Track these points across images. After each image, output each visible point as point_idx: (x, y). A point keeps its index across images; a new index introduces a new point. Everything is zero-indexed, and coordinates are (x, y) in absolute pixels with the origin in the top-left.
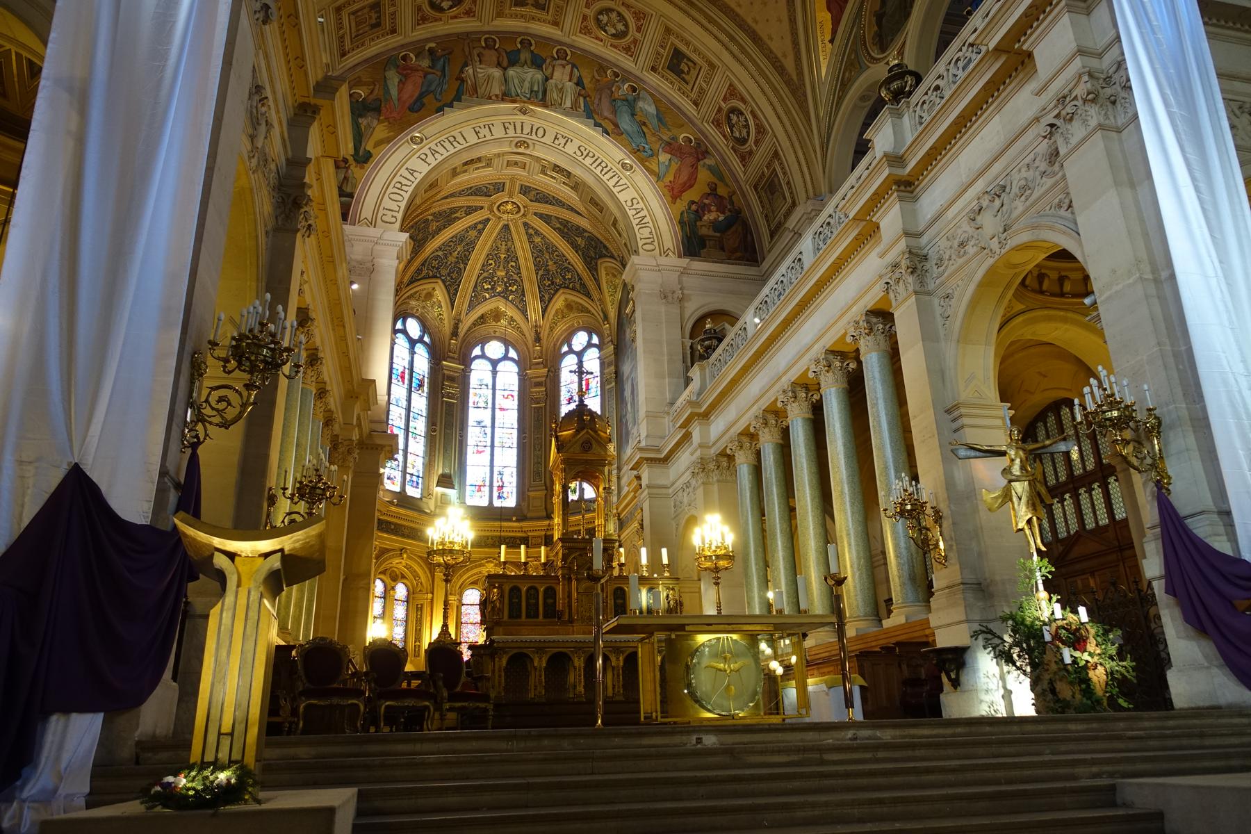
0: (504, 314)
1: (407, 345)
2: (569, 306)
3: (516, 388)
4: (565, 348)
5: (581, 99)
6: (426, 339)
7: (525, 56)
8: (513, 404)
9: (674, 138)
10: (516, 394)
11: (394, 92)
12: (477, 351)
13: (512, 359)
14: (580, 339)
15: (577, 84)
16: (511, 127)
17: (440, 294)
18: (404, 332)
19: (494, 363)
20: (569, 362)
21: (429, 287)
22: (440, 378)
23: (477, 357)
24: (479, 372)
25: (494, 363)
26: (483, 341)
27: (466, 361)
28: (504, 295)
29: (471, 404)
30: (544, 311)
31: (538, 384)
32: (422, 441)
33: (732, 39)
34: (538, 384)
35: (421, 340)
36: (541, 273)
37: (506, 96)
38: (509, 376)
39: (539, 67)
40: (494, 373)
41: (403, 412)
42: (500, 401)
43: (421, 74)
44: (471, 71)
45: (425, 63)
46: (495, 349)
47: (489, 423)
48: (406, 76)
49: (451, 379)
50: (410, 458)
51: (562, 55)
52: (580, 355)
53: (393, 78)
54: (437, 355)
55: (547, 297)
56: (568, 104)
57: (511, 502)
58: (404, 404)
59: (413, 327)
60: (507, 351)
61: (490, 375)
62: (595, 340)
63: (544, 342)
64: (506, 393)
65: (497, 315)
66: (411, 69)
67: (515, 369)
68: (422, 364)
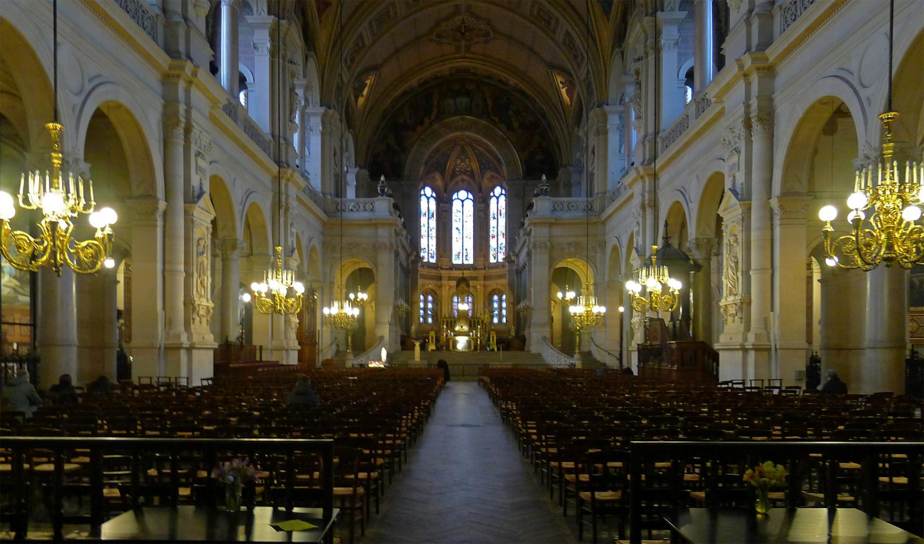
2: (492, 177)
6: (434, 195)
12: (455, 196)
14: (498, 190)
17: (438, 176)
19: (463, 201)
20: (493, 201)
24: (456, 205)
25: (463, 201)
27: (450, 202)
31: (481, 211)
32: (435, 239)
34: (481, 211)
38: (469, 205)
46: (463, 194)
47: (461, 228)
49: (445, 211)
52: (498, 198)
54: (439, 200)
59: (428, 191)
62: (504, 192)
65: (463, 181)
67: (471, 203)
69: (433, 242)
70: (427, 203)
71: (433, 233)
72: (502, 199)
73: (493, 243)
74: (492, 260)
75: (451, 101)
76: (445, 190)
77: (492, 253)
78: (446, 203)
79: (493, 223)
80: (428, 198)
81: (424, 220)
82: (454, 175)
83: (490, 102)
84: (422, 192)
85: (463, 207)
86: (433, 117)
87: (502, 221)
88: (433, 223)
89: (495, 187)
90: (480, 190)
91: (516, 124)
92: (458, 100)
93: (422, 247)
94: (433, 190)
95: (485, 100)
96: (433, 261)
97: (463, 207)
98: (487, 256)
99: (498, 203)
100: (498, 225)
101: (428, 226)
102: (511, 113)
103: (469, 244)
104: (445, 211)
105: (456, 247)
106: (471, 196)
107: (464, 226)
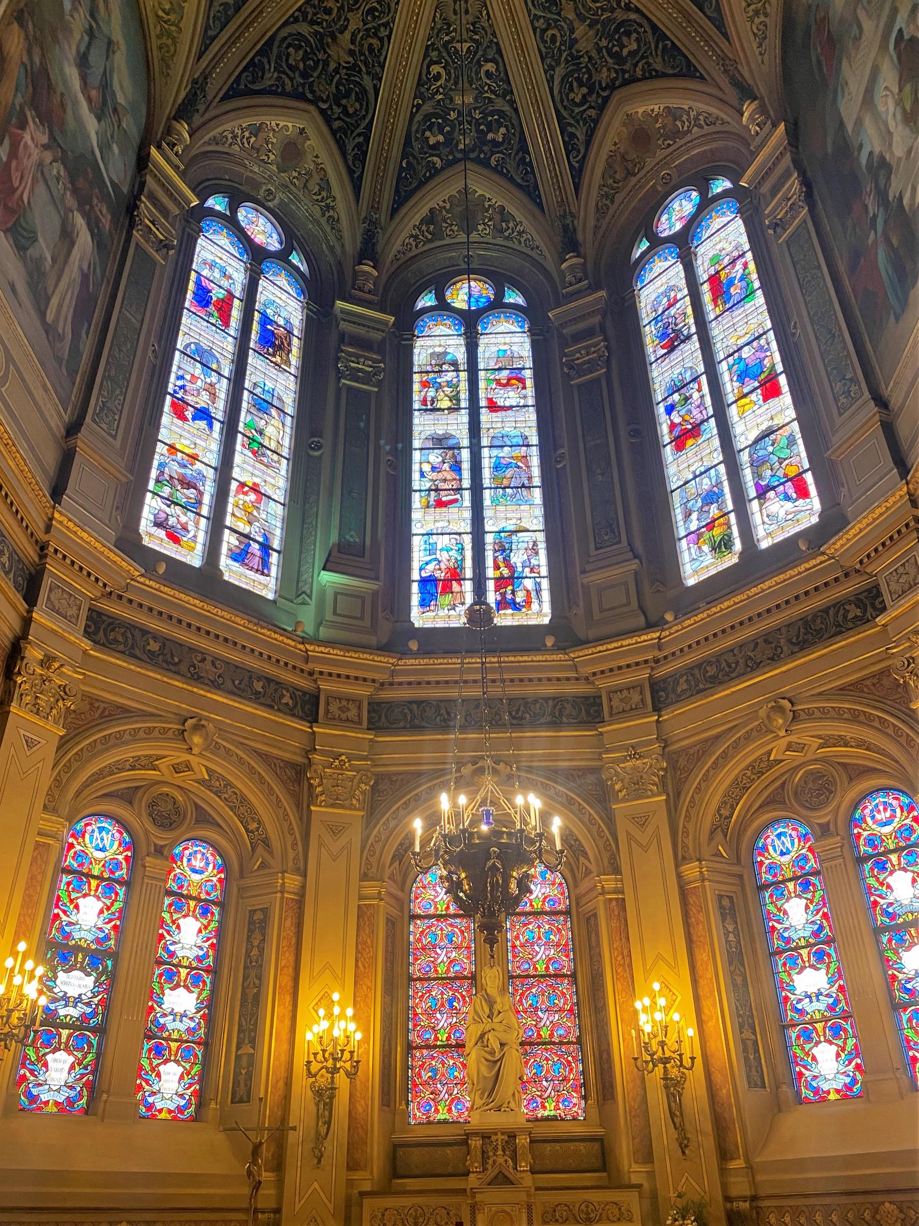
25: (470, 323)
26: (440, 284)
28: (479, 156)
30: (577, 174)
36: (559, 72)
55: (581, 134)
57: (540, 613)
60: (500, 294)
85: (475, 377)
97: (475, 377)
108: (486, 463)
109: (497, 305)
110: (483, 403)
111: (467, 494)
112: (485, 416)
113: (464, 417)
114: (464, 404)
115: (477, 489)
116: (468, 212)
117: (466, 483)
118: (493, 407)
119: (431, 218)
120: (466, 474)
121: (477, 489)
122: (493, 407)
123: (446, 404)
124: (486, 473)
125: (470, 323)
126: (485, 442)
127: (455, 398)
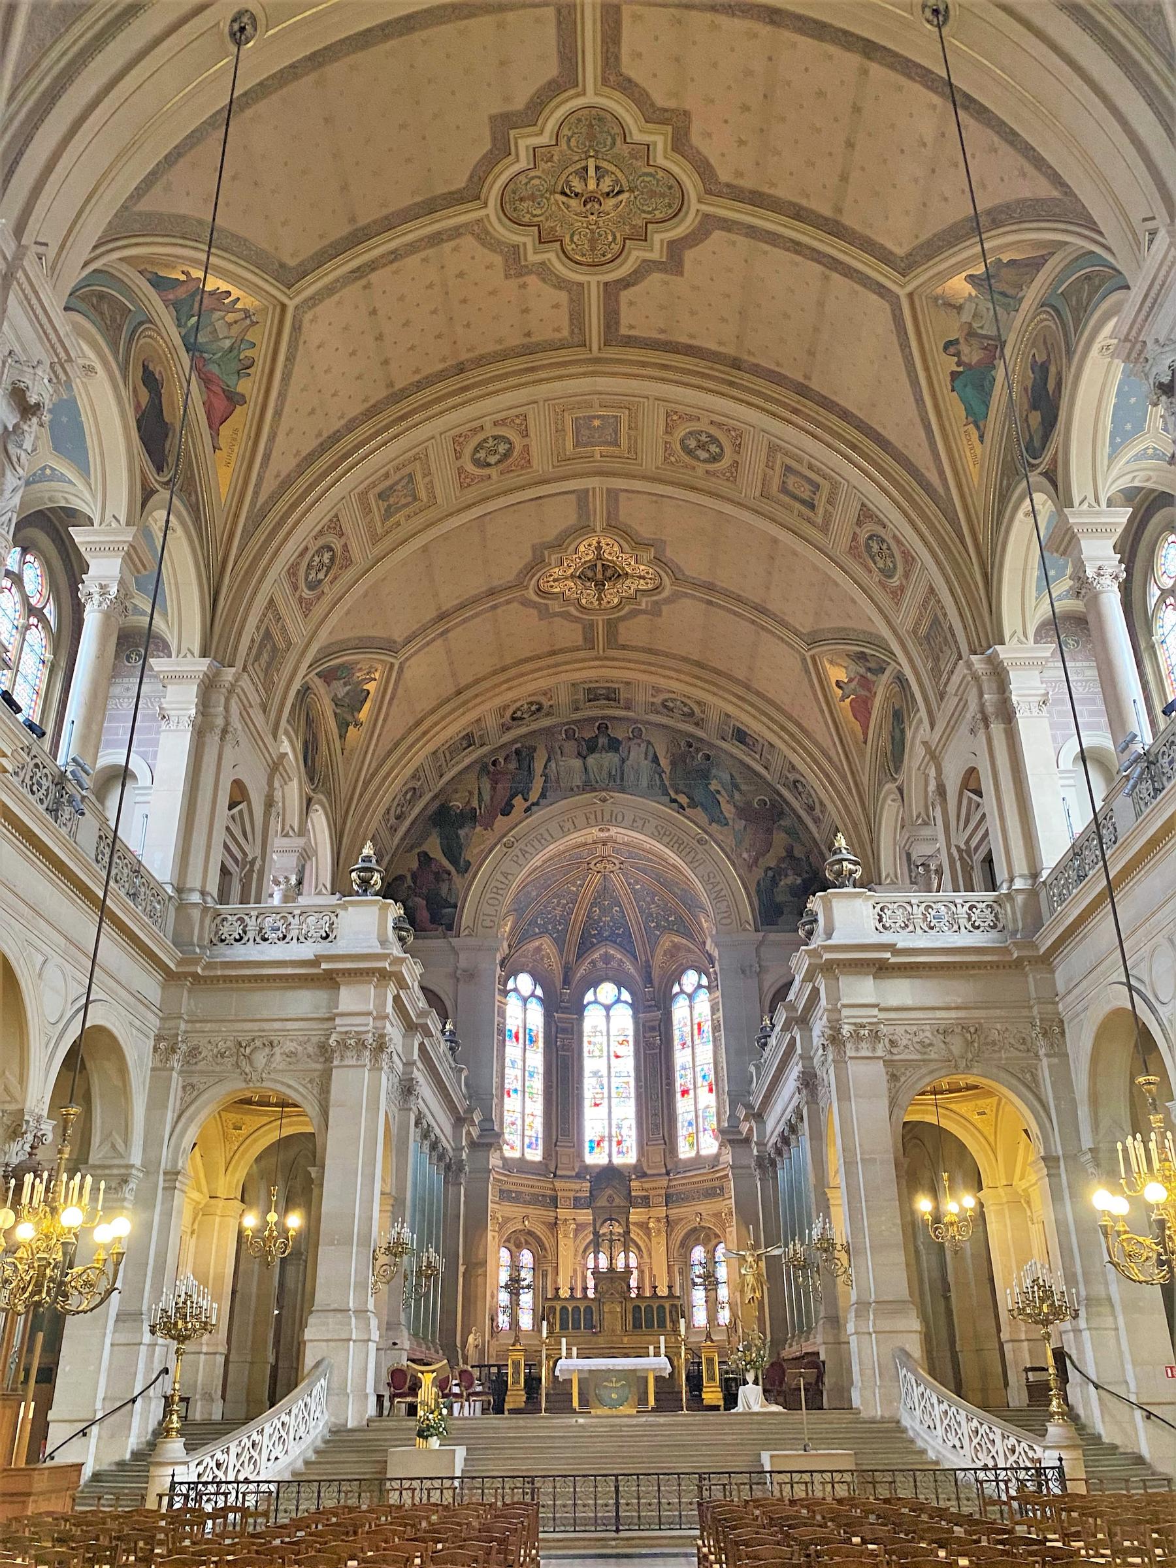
0: (613, 956)
1: (520, 1003)
3: (630, 1032)
4: (676, 989)
5: (657, 776)
6: (539, 992)
7: (602, 741)
8: (628, 1051)
9: (749, 804)
10: (631, 1039)
11: (487, 797)
12: (589, 997)
13: (626, 1002)
14: (690, 979)
15: (653, 761)
16: (593, 817)
18: (515, 990)
21: (537, 943)
22: (553, 1030)
23: (589, 1003)
24: (593, 1019)
25: (608, 1008)
27: (580, 1009)
29: (586, 1054)
31: (653, 1029)
32: (540, 1100)
33: (783, 728)
34: (653, 1029)
35: (533, 995)
37: (588, 786)
38: (624, 1019)
39: (617, 750)
40: (608, 1017)
41: (519, 1073)
42: (615, 1047)
43: (510, 777)
44: (554, 766)
45: (513, 765)
46: (607, 991)
48: (495, 782)
49: (564, 1031)
50: (528, 1120)
51: (637, 734)
52: (690, 997)
53: (486, 785)
54: (550, 1005)
56: (644, 783)
58: (520, 1064)
59: (524, 982)
61: (604, 1019)
62: (704, 981)
63: (656, 984)
64: (621, 1039)
66: (501, 773)
67: (629, 1012)
68: (536, 1017)
69: (536, 1106)
70: (522, 1010)
71: (537, 1084)
72: (703, 995)
73: (683, 1106)
74: (685, 1152)
75: (577, 763)
76: (566, 982)
77: (682, 1131)
78: (565, 1010)
79: (681, 1057)
80: (525, 1000)
81: (513, 1051)
82: (584, 947)
83: (663, 762)
84: (510, 985)
85: (608, 1023)
86: (534, 796)
87: (705, 1053)
88: (536, 1059)
89: (683, 972)
90: (649, 980)
91: (728, 810)
92: (590, 760)
93: (508, 1119)
94: (537, 980)
95: (655, 760)
96: (535, 1155)
97: (608, 1023)
98: (670, 1143)
99: (694, 1008)
100: (696, 1058)
101: (523, 1067)
102: (714, 786)
103: (626, 1111)
104: (564, 1031)
105: (593, 1123)
106: (626, 996)
107: (611, 1075)
108: (613, 1086)
109: (618, 1001)
110: (612, 1054)
111: (606, 1100)
112: (613, 1058)
113: (605, 1058)
114: (605, 1054)
115: (610, 1097)
116: (607, 958)
117: (606, 1095)
118: (617, 1057)
119: (593, 962)
120: (606, 1091)
121: (610, 1097)
122: (617, 1057)
123: (597, 1053)
124: (613, 1091)
125: (608, 1008)
126: (613, 1074)
127: (601, 1050)
